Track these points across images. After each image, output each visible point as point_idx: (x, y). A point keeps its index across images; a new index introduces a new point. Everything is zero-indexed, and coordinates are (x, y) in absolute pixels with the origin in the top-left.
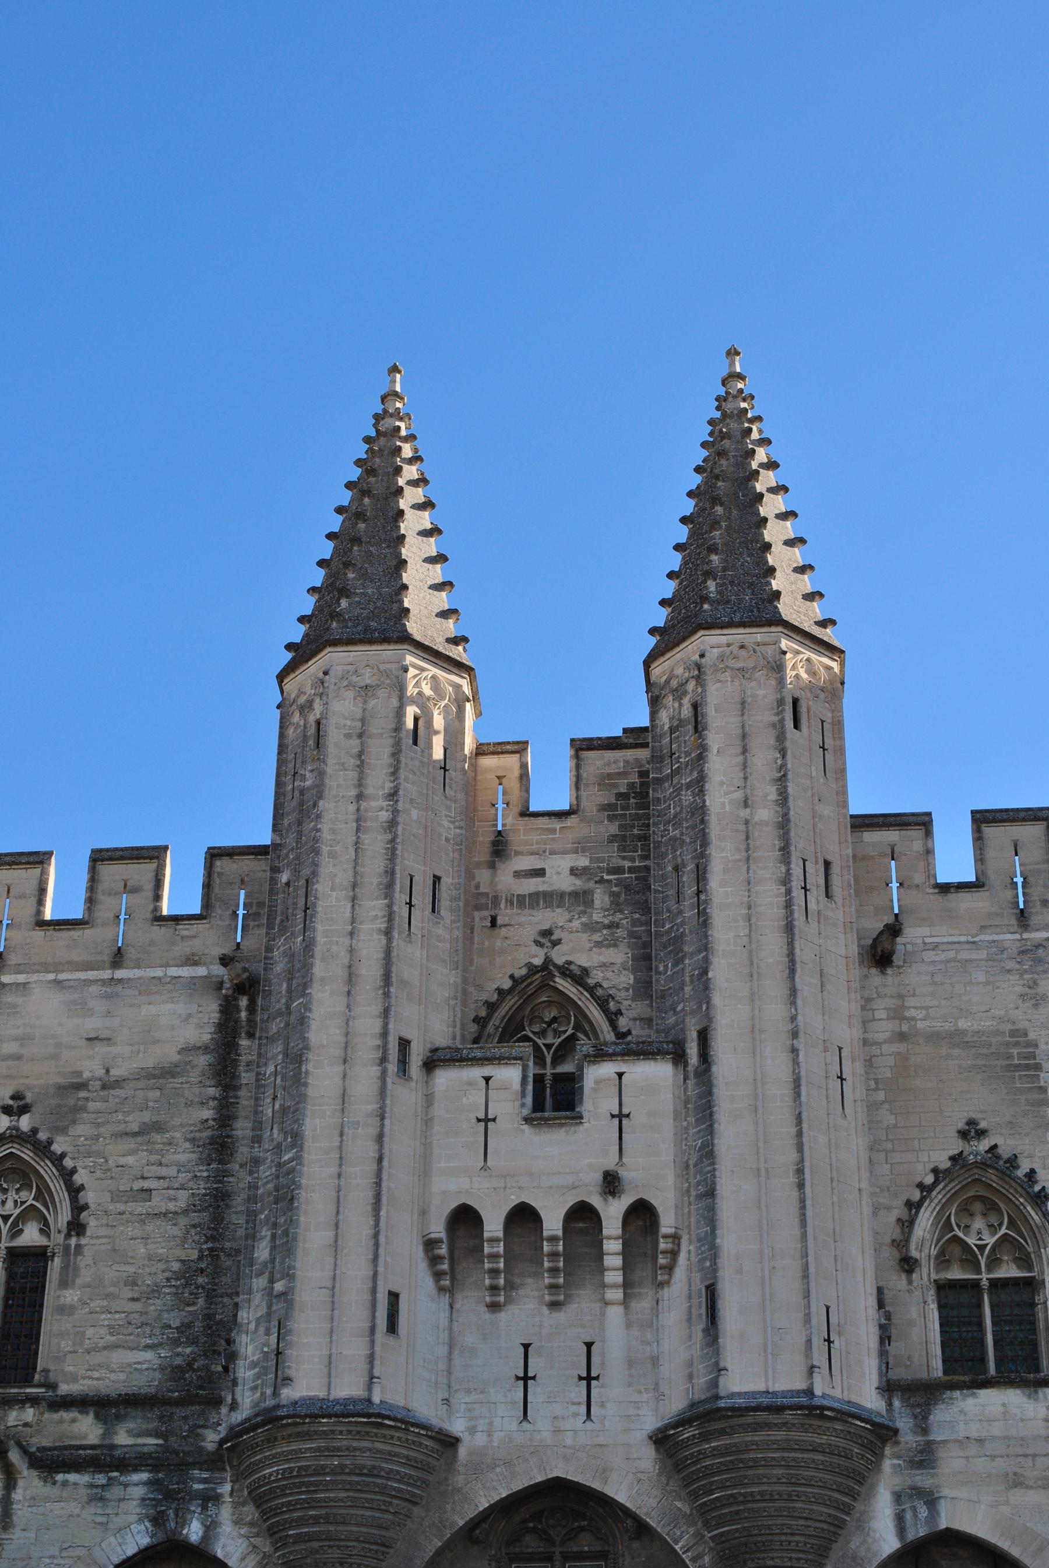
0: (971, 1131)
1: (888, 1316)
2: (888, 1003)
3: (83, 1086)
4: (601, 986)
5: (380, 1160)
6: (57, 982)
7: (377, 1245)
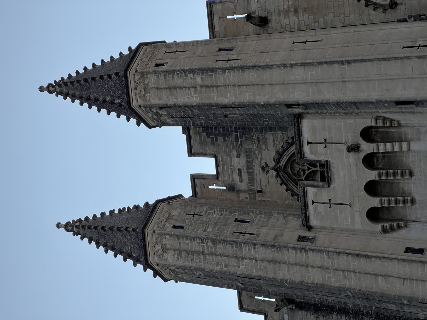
1: (410, 17)
2: (282, 18)
4: (283, 146)
7: (383, 257)
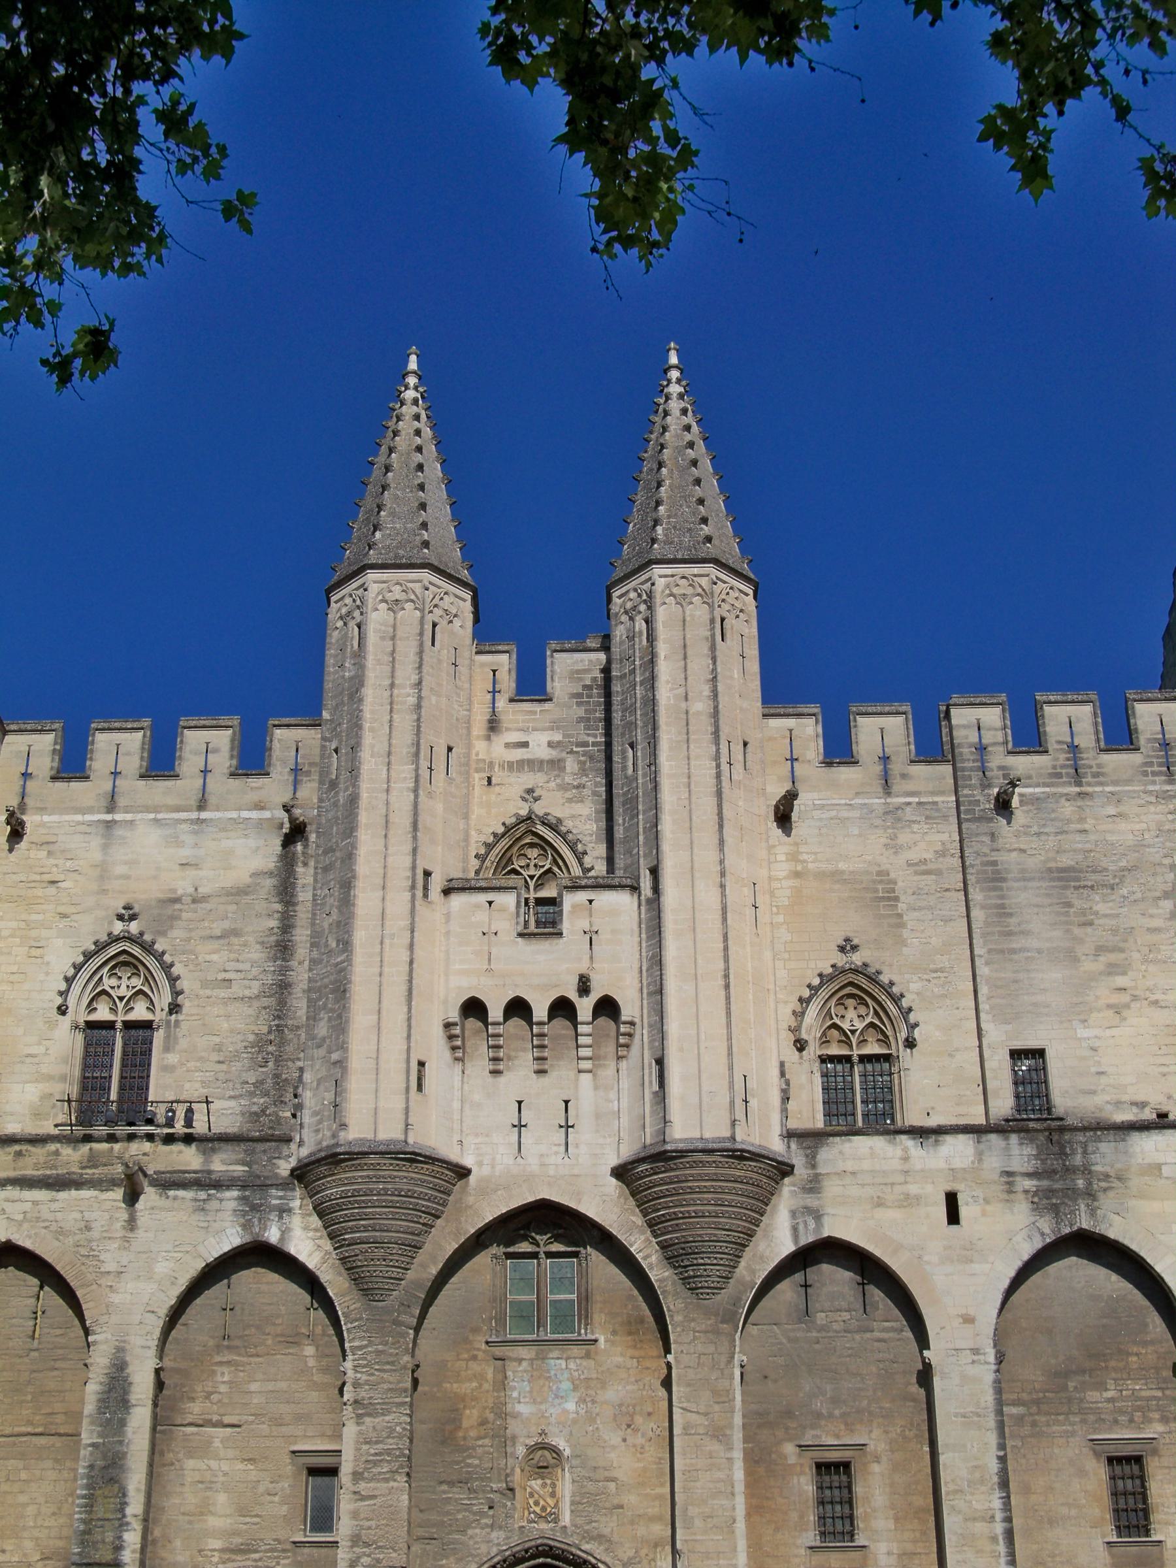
0: (847, 947)
1: (788, 1083)
2: (786, 849)
3: (177, 900)
5: (411, 962)
6: (156, 820)
7: (409, 1026)
